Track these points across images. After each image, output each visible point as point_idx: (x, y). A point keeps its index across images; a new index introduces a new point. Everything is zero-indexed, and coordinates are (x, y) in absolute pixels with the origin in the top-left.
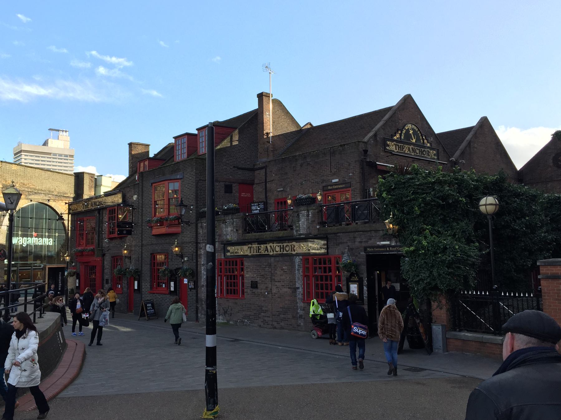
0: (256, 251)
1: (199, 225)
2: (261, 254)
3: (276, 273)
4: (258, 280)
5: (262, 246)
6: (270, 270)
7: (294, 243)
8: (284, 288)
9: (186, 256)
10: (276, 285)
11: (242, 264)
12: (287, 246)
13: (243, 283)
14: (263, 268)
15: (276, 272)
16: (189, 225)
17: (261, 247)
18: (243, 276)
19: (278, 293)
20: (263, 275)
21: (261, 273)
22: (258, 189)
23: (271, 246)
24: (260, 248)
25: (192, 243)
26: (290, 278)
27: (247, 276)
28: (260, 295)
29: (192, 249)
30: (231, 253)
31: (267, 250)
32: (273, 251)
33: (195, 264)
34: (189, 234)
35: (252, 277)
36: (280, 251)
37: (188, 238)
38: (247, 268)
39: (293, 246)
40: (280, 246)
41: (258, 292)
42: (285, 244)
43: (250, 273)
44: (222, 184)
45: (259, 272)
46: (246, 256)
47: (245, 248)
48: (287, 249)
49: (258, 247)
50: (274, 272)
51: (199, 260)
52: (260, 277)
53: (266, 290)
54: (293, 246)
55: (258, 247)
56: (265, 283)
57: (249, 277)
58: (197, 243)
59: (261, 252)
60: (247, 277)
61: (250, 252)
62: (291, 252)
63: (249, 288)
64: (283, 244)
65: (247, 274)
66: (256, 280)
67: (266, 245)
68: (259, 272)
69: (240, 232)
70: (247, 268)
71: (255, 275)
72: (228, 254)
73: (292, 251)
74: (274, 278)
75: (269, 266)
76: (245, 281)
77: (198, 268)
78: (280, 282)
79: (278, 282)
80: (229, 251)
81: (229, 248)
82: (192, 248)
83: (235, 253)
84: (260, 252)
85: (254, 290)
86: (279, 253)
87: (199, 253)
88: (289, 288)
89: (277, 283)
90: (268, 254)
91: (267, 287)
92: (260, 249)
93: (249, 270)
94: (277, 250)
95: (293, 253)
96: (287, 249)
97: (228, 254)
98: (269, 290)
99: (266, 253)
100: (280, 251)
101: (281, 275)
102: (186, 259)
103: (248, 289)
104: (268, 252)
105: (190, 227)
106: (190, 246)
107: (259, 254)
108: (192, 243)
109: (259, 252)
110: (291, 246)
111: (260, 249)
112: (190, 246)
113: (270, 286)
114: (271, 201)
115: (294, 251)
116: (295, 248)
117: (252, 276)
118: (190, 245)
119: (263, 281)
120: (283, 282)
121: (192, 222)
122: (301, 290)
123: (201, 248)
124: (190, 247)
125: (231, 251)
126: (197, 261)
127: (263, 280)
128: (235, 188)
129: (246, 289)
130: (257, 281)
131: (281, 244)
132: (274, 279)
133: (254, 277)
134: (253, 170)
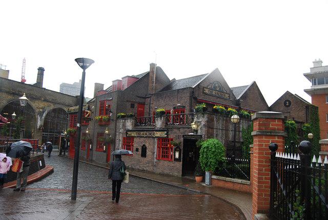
22: (147, 107)
44: (130, 103)
47: (135, 133)
114: (152, 113)
122: (156, 153)
128: (136, 105)
134: (145, 98)
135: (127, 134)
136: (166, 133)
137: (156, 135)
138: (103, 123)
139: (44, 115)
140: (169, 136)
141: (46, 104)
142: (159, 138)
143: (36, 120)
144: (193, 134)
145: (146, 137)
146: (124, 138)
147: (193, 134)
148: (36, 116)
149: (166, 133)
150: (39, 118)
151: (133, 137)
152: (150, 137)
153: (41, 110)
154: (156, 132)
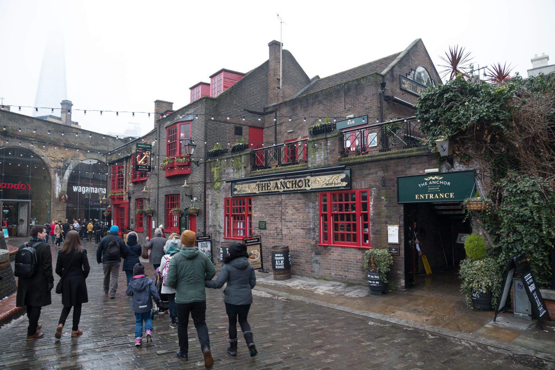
0: (265, 189)
2: (270, 191)
3: (287, 212)
4: (266, 219)
5: (272, 182)
6: (280, 209)
7: (309, 177)
8: (297, 228)
9: (195, 197)
10: (287, 226)
11: (250, 203)
13: (250, 223)
14: (272, 207)
15: (287, 210)
16: (198, 166)
18: (250, 216)
19: (289, 234)
20: (272, 215)
21: (269, 213)
23: (281, 182)
26: (303, 217)
27: (255, 215)
28: (268, 236)
29: (201, 189)
30: (238, 192)
31: (277, 187)
32: (284, 188)
33: (203, 204)
35: (260, 217)
36: (292, 187)
38: (255, 207)
39: (307, 182)
40: (292, 181)
41: (266, 234)
42: (298, 180)
43: (258, 212)
45: (268, 211)
46: (255, 195)
47: (253, 185)
48: (300, 184)
49: (267, 184)
50: (285, 211)
51: (207, 199)
52: (269, 217)
53: (275, 231)
56: (274, 224)
57: (257, 217)
59: (270, 189)
60: (254, 217)
61: (259, 190)
62: (304, 188)
64: (296, 179)
65: (255, 214)
66: (265, 220)
67: (275, 182)
68: (268, 211)
69: (249, 168)
70: (255, 207)
71: (264, 215)
72: (235, 193)
73: (306, 186)
74: (284, 217)
75: (280, 204)
76: (253, 221)
77: (207, 208)
78: (292, 222)
79: (289, 222)
80: (236, 190)
81: (236, 187)
83: (243, 191)
84: (269, 189)
85: (262, 231)
86: (291, 189)
87: (207, 193)
88: (302, 229)
89: (288, 224)
90: (278, 192)
91: (276, 228)
92: (269, 186)
93: (257, 209)
94: (288, 186)
95: (308, 188)
96: (300, 184)
97: (235, 193)
98: (279, 230)
99: (276, 190)
100: (292, 187)
101: (293, 215)
102: (195, 199)
104: (278, 189)
105: (199, 167)
106: (199, 186)
107: (268, 191)
108: (201, 183)
109: (267, 189)
110: (305, 180)
111: (269, 186)
112: (199, 186)
113: (280, 226)
115: (309, 186)
116: (310, 184)
117: (260, 215)
118: (199, 185)
119: (272, 221)
120: (296, 222)
121: (201, 162)
124: (199, 188)
125: (238, 189)
126: (205, 201)
127: (273, 220)
129: (254, 229)
130: (265, 222)
132: (285, 219)
133: (262, 217)
135: (233, 190)
136: (343, 176)
138: (176, 171)
139: (67, 173)
140: (354, 184)
141: (69, 153)
142: (322, 192)
143: (50, 183)
144: (436, 170)
145: (285, 193)
146: (227, 200)
147: (436, 170)
148: (52, 176)
149: (343, 176)
150: (58, 179)
151: (250, 197)
152: (295, 192)
153: (61, 164)
154: (312, 179)
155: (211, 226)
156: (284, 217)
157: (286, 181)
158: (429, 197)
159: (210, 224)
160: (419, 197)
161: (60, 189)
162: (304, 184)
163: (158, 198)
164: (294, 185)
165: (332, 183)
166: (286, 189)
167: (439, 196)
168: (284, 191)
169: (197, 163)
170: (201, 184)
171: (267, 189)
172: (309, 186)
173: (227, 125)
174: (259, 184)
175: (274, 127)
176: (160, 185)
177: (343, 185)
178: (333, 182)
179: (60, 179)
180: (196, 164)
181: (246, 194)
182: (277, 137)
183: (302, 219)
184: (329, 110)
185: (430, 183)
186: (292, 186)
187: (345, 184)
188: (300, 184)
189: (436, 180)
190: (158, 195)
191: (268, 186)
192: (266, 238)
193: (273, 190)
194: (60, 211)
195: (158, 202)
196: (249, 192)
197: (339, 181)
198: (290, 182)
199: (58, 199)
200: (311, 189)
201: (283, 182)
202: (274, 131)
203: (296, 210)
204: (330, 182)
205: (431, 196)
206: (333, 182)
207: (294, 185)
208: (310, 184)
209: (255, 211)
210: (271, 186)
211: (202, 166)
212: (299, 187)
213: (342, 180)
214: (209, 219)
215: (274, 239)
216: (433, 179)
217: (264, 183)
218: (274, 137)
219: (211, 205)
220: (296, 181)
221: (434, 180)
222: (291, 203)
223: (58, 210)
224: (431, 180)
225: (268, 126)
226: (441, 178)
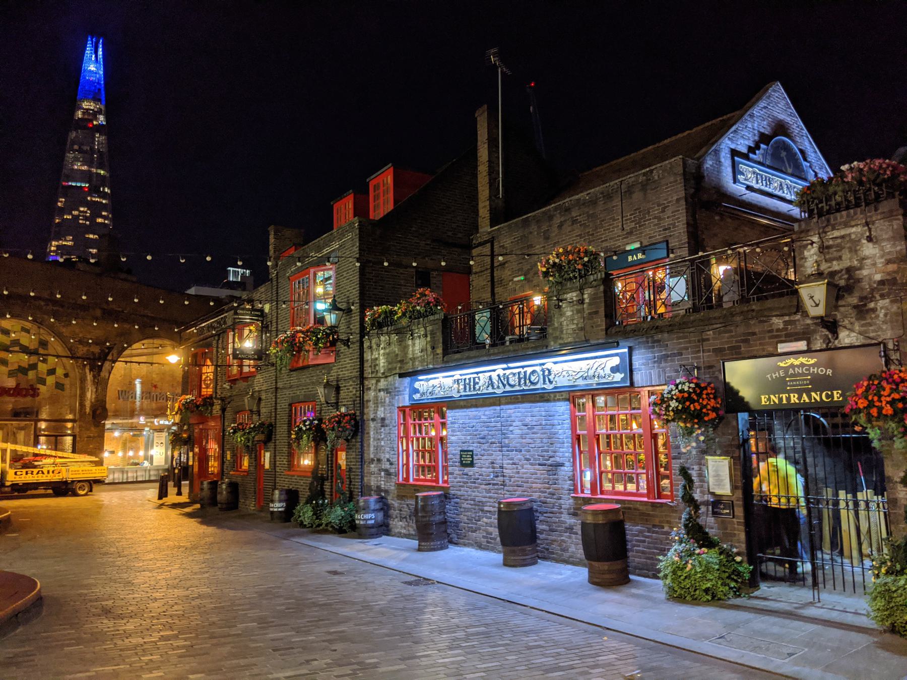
0: (470, 388)
1: (366, 345)
2: (479, 392)
9: (344, 405)
12: (533, 372)
15: (511, 428)
16: (348, 346)
17: (479, 378)
19: (517, 475)
23: (499, 376)
24: (477, 380)
25: (354, 379)
28: (478, 479)
31: (492, 384)
32: (504, 386)
34: (349, 363)
36: (519, 385)
37: (348, 370)
38: (452, 423)
39: (547, 373)
40: (519, 373)
42: (529, 370)
49: (474, 379)
51: (366, 411)
54: (547, 373)
55: (474, 379)
58: (362, 378)
59: (479, 390)
62: (543, 386)
63: (457, 464)
64: (525, 369)
66: (471, 448)
70: (452, 423)
75: (498, 417)
78: (521, 451)
80: (416, 391)
82: (353, 388)
84: (477, 387)
85: (467, 470)
86: (517, 388)
87: (366, 398)
88: (540, 465)
90: (494, 393)
91: (493, 463)
92: (478, 383)
93: (456, 426)
94: (512, 383)
95: (549, 387)
97: (417, 396)
99: (490, 390)
100: (519, 385)
103: (456, 466)
104: (493, 388)
106: (351, 385)
109: (474, 388)
111: (478, 383)
112: (351, 385)
115: (551, 382)
116: (551, 377)
118: (351, 383)
123: (369, 389)
124: (351, 388)
125: (421, 390)
127: (485, 446)
130: (472, 451)
131: (521, 370)
137: (562, 382)
155: (373, 460)
156: (507, 441)
157: (508, 372)
158: (788, 399)
159: (372, 456)
160: (769, 399)
161: (94, 396)
162: (542, 377)
163: (276, 409)
164: (523, 381)
165: (594, 376)
166: (508, 388)
167: (810, 397)
168: (504, 392)
169: (347, 343)
170: (354, 382)
171: (474, 388)
172: (551, 382)
173: (401, 271)
174: (458, 380)
175: (489, 271)
176: (280, 385)
177: (615, 380)
178: (596, 374)
179: (94, 376)
180: (344, 344)
181: (436, 398)
182: (496, 289)
183: (540, 445)
184: (593, 234)
185: (791, 371)
186: (519, 382)
187: (618, 377)
188: (533, 378)
189: (802, 365)
190: (276, 404)
191: (475, 383)
192: (475, 483)
193: (485, 391)
194: (94, 437)
195: (276, 417)
196: (442, 394)
197: (607, 370)
198: (514, 374)
199: (89, 414)
200: (555, 388)
201: (501, 375)
202: (489, 278)
203: (528, 429)
204: (591, 373)
205: (794, 399)
206: (596, 374)
207: (523, 381)
208: (551, 377)
209: (453, 431)
210: (480, 384)
211: (356, 346)
212: (532, 383)
213: (614, 370)
214: (369, 445)
215: (490, 484)
216: (797, 362)
217: (467, 377)
218: (489, 289)
219: (373, 420)
220: (525, 372)
221: (798, 366)
222: (519, 414)
223: (90, 437)
224: (792, 366)
225: (478, 270)
226: (812, 361)
